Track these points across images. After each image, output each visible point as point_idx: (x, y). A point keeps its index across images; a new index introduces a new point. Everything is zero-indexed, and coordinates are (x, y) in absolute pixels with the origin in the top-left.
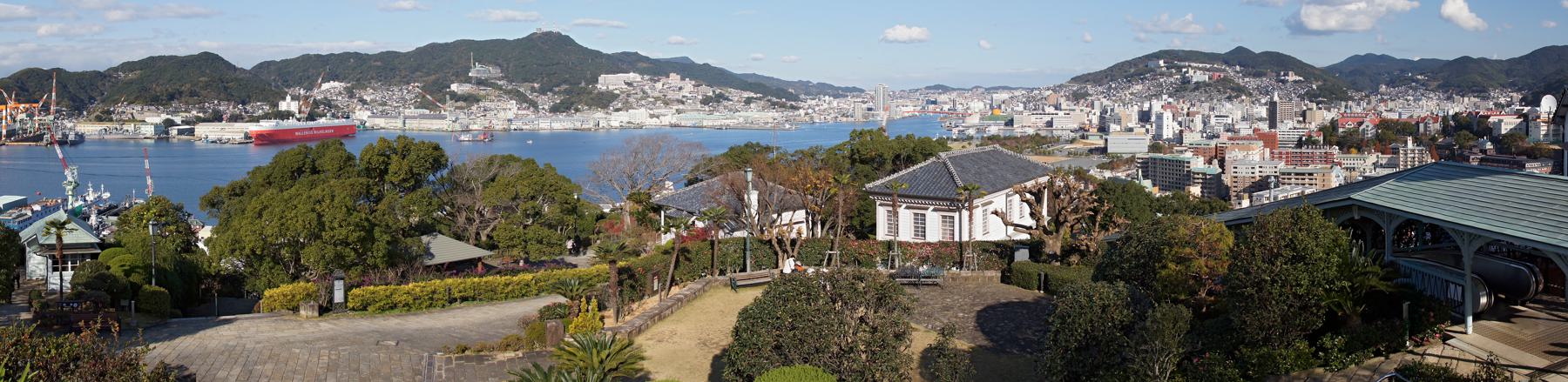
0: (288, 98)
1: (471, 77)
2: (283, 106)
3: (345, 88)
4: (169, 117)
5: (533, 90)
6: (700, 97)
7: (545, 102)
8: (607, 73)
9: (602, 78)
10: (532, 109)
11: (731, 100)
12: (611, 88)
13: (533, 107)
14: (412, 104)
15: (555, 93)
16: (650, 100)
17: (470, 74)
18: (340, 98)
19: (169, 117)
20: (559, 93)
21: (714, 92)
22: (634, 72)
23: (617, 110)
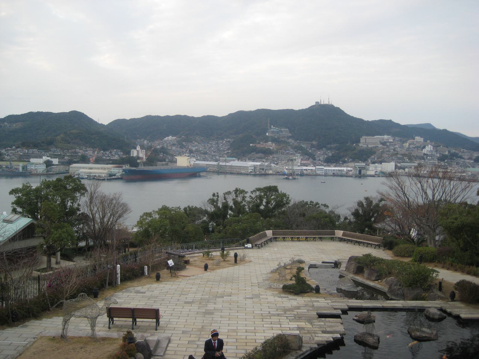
0: (138, 148)
1: (268, 137)
2: (134, 153)
3: (177, 142)
4: (49, 158)
5: (313, 146)
6: (438, 155)
7: (320, 155)
8: (368, 135)
9: (362, 140)
10: (311, 160)
11: (463, 158)
12: (370, 146)
13: (312, 158)
14: (226, 154)
15: (328, 149)
17: (267, 134)
18: (174, 148)
19: (49, 158)
20: (330, 149)
21: (449, 152)
22: (388, 135)
23: (374, 163)
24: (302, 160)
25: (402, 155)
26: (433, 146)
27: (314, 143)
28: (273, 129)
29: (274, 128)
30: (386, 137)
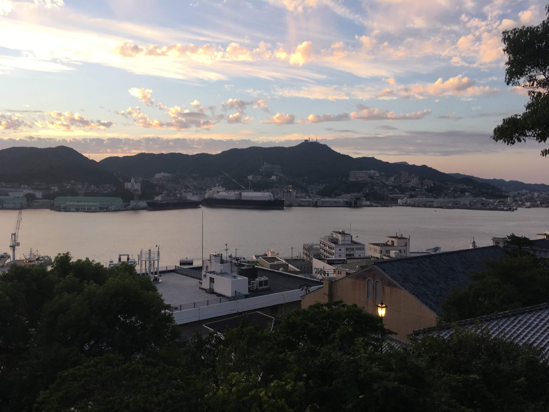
12: (359, 179)
16: (390, 188)
21: (434, 184)
24: (297, 193)
25: (393, 186)
26: (419, 179)
27: (306, 178)
28: (266, 165)
29: (267, 164)
30: (372, 171)
